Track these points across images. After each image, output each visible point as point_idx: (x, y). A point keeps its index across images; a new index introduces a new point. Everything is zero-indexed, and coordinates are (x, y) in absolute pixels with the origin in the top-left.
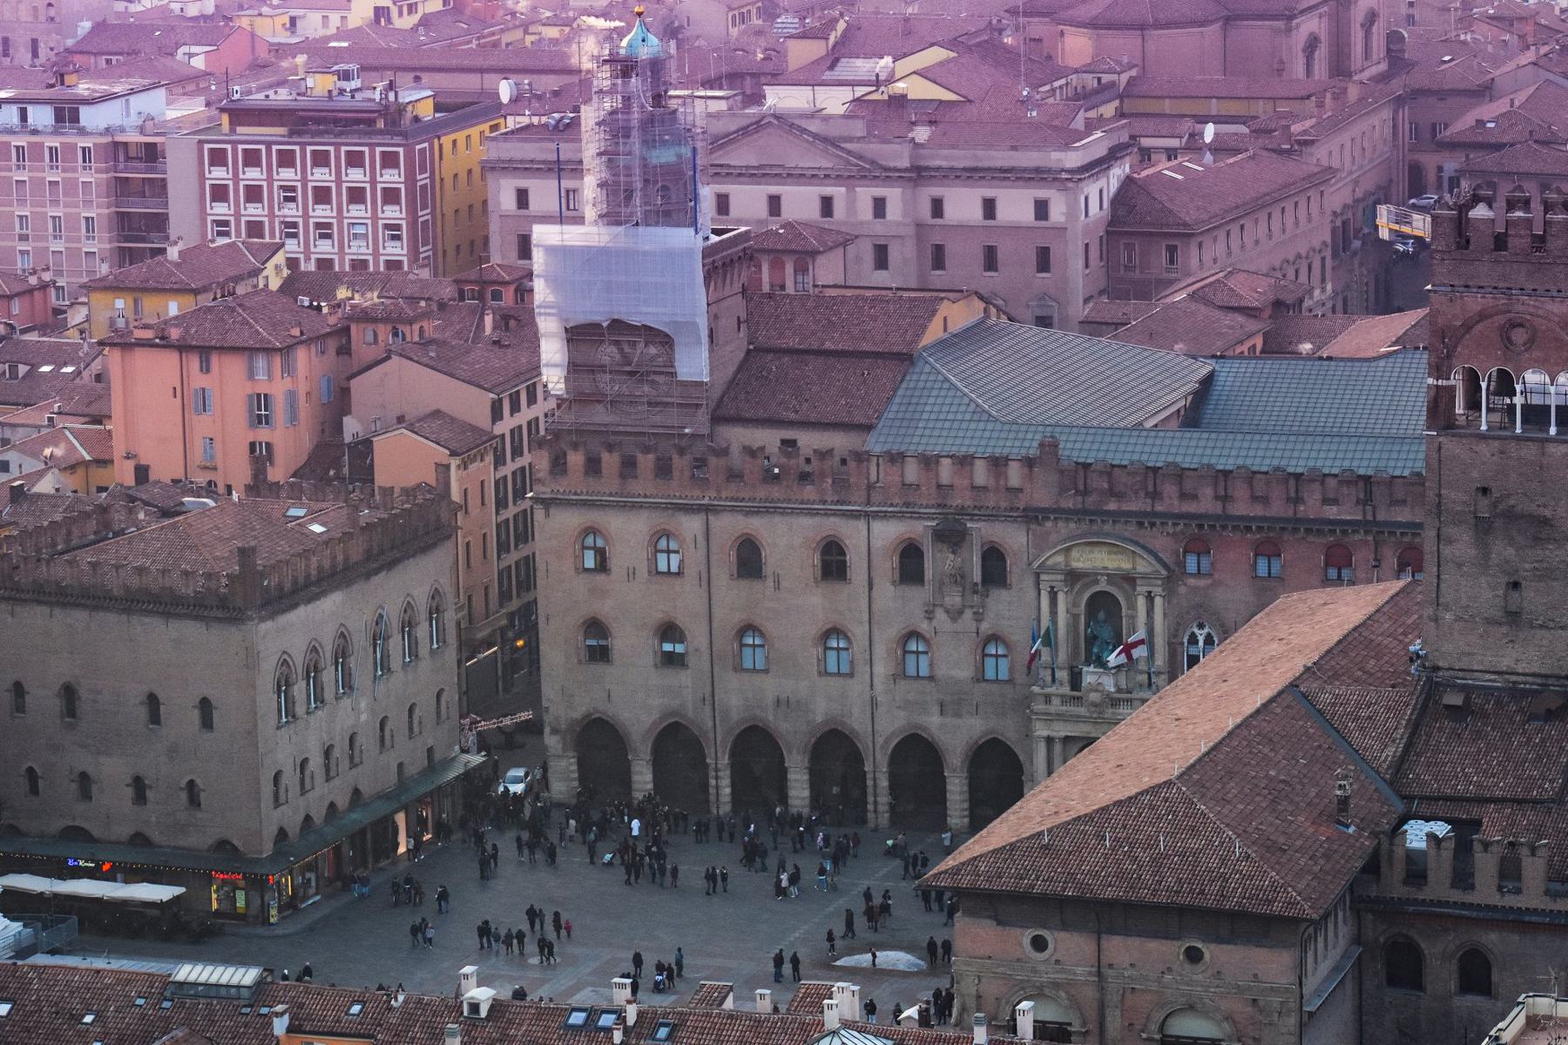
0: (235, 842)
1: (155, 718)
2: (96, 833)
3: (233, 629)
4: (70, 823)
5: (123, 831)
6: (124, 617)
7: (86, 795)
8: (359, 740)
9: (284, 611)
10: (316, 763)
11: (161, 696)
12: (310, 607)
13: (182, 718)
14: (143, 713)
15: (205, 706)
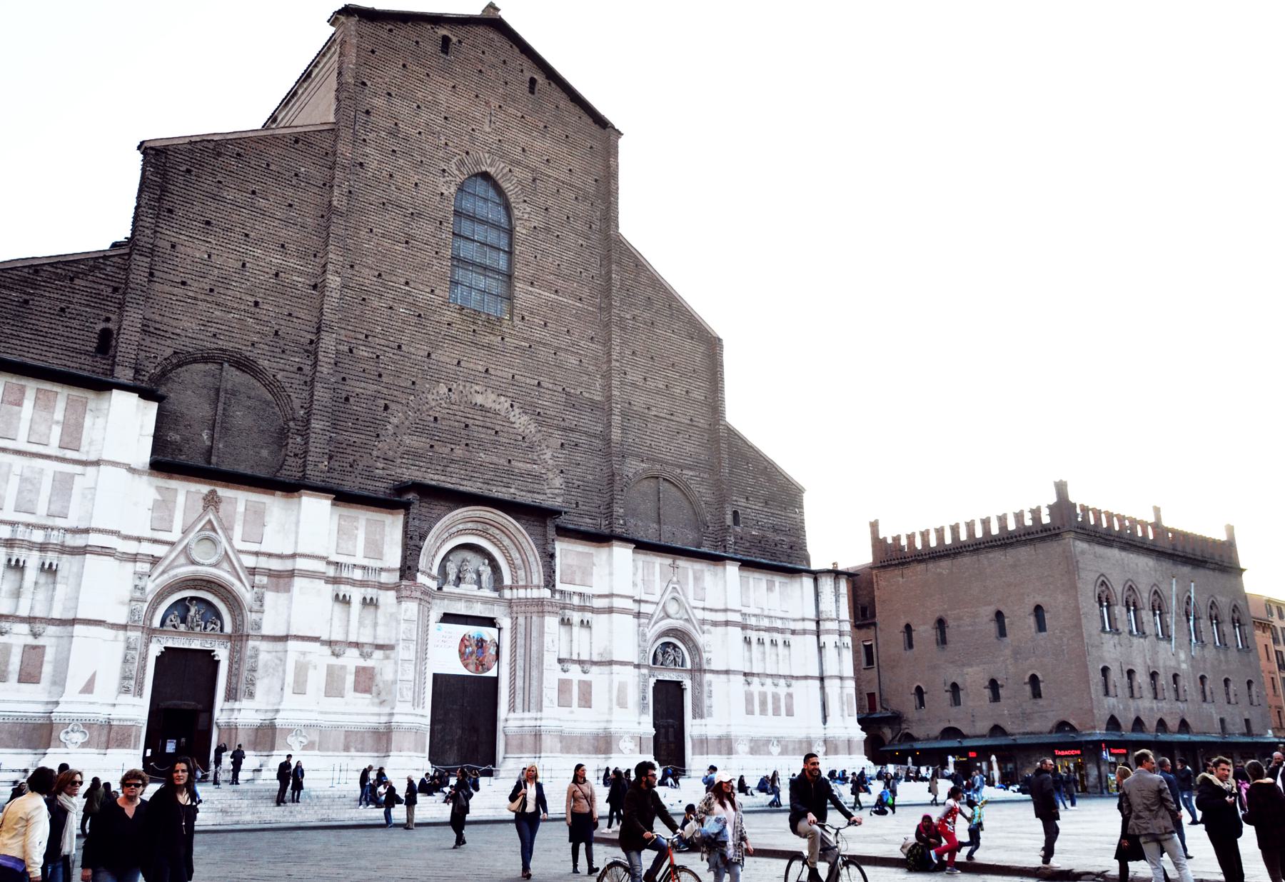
0: (1073, 722)
1: (1002, 633)
2: (965, 731)
3: (1055, 544)
4: (947, 725)
5: (984, 726)
6: (975, 557)
7: (956, 701)
8: (1181, 682)
9: (1099, 543)
10: (1142, 678)
11: (1005, 612)
12: (1124, 554)
13: (1020, 623)
14: (993, 627)
15: (1038, 610)
